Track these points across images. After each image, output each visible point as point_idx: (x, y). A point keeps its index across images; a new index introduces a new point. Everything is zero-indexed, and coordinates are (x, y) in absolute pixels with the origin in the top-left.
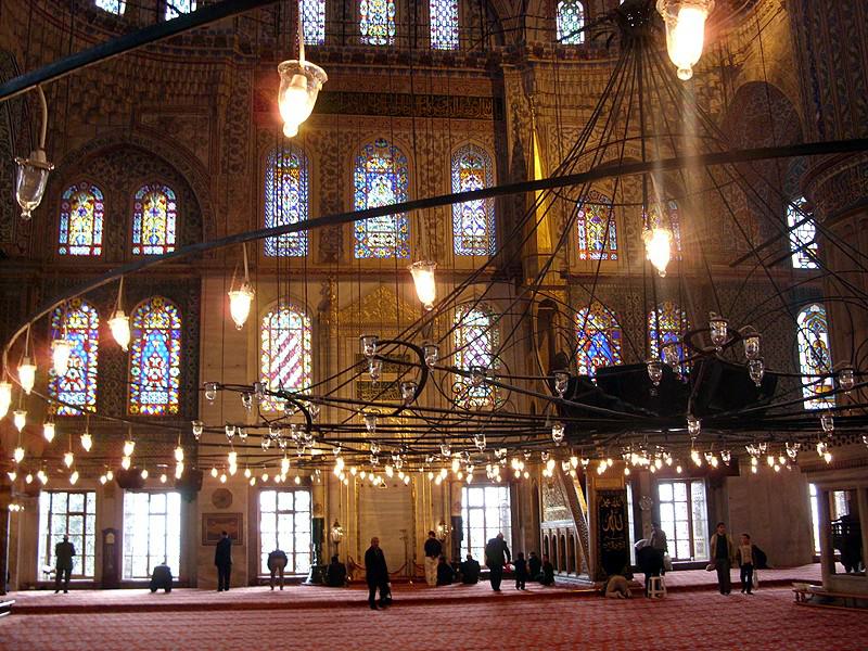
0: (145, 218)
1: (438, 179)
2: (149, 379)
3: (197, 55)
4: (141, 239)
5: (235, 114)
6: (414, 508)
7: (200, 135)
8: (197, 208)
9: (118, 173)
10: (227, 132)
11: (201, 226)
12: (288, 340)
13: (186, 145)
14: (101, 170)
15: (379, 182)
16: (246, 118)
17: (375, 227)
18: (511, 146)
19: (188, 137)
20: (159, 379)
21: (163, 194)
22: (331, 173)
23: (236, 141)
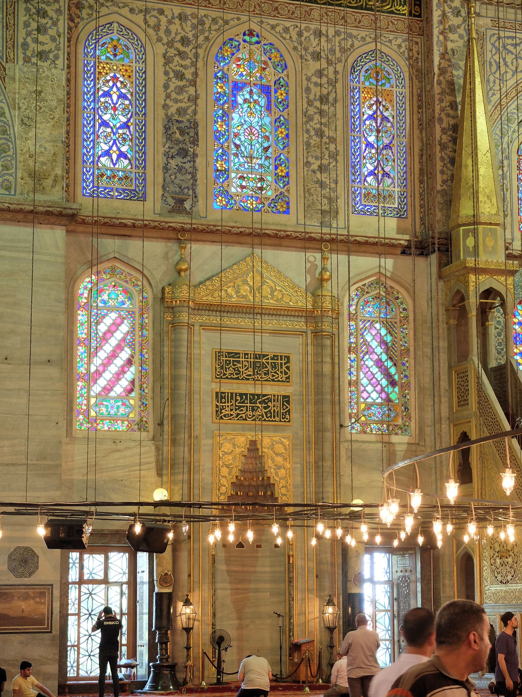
1: (331, 99)
12: (116, 325)
15: (247, 96)
22: (180, 76)
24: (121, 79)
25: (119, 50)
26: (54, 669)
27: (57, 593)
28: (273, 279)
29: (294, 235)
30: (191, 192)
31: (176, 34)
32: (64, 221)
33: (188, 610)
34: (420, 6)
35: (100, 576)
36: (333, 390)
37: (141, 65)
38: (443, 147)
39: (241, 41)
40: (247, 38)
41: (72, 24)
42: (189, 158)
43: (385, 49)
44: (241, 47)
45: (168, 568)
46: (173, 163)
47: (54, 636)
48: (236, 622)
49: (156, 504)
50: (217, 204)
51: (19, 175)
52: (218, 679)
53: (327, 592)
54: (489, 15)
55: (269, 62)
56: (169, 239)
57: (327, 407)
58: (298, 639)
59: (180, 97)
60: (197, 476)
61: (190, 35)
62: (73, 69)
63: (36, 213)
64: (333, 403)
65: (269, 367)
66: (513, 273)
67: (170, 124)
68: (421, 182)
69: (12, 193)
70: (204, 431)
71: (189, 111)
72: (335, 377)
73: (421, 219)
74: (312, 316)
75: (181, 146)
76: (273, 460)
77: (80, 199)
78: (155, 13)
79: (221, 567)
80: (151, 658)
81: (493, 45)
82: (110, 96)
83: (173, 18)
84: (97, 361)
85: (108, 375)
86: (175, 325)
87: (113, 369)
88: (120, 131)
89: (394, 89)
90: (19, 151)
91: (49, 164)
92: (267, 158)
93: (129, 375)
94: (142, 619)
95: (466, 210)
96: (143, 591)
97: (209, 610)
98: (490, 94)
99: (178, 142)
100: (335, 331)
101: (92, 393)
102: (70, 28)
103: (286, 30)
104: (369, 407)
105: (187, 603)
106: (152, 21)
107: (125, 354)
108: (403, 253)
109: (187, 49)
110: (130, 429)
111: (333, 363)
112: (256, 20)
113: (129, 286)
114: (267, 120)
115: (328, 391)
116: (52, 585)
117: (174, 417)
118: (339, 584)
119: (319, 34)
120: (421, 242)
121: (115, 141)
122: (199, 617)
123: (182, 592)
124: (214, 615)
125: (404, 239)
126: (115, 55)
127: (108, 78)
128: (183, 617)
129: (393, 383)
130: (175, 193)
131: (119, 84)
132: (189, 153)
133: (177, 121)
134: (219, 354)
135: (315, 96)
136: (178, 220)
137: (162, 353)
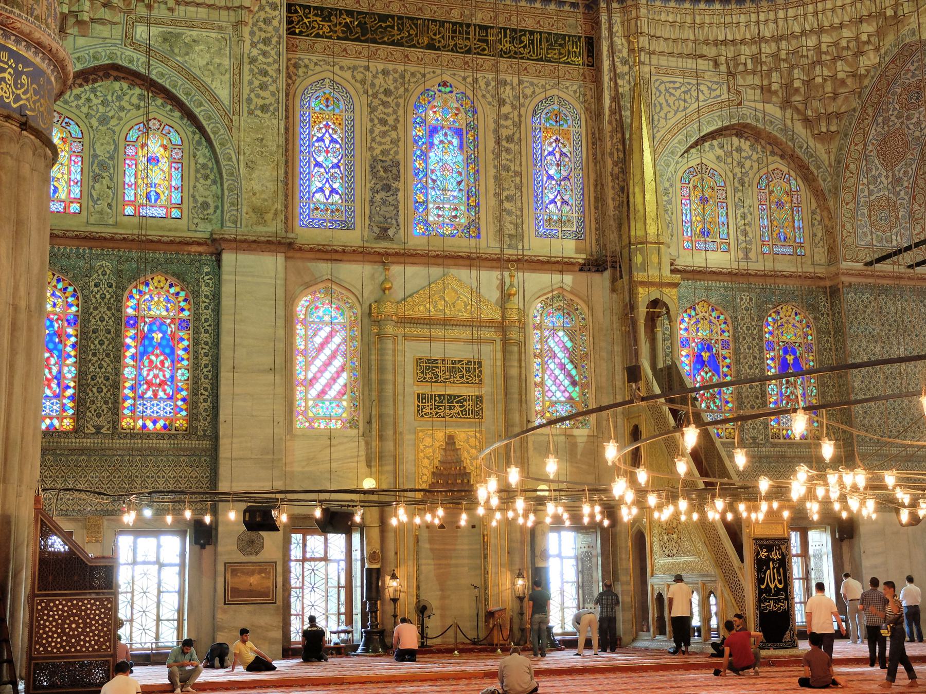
2: (149, 384)
5: (263, 35)
6: (485, 557)
7: (217, 60)
9: (103, 103)
10: (253, 61)
12: (330, 336)
13: (198, 73)
14: (78, 97)
15: (442, 138)
16: (279, 43)
18: (607, 102)
19: (202, 62)
20: (162, 384)
22: (383, 122)
23: (265, 73)
25: (331, 102)
26: (278, 634)
27: (280, 569)
28: (466, 294)
29: (484, 256)
30: (394, 222)
31: (380, 87)
32: (283, 249)
33: (394, 583)
34: (592, 57)
35: (321, 555)
36: (520, 392)
37: (350, 114)
38: (615, 177)
40: (443, 89)
41: (290, 81)
42: (391, 192)
43: (562, 95)
45: (377, 547)
46: (378, 197)
47: (278, 606)
48: (439, 593)
49: (365, 492)
50: (419, 230)
51: (244, 210)
52: (423, 643)
53: (517, 567)
55: (461, 108)
56: (376, 262)
57: (515, 405)
58: (492, 607)
59: (384, 140)
60: (401, 467)
61: (392, 88)
62: (291, 119)
64: (521, 401)
65: (464, 372)
66: (676, 285)
68: (596, 208)
70: (406, 428)
71: (392, 152)
72: (523, 379)
73: (597, 240)
74: (502, 327)
75: (385, 182)
76: (468, 452)
77: (297, 229)
78: (362, 69)
79: (425, 546)
80: (364, 625)
81: (657, 89)
82: (323, 141)
83: (377, 73)
84: (314, 369)
85: (323, 381)
86: (381, 337)
87: (327, 375)
88: (332, 171)
89: (571, 129)
90: (244, 190)
91: (270, 201)
92: (460, 190)
93: (342, 381)
94: (356, 591)
95: (636, 231)
96: (357, 567)
97: (414, 583)
98: (655, 131)
99: (382, 179)
100: (522, 339)
101: (309, 396)
102: (288, 85)
104: (553, 404)
105: (394, 577)
106: (359, 77)
107: (338, 363)
108: (581, 270)
109: (390, 100)
110: (344, 427)
111: (520, 367)
112: (449, 73)
113: (341, 304)
114: (460, 158)
115: (515, 389)
116: (276, 563)
117: (381, 416)
118: (528, 559)
120: (596, 260)
122: (405, 589)
123: (389, 568)
124: (418, 587)
125: (581, 258)
126: (327, 106)
127: (321, 126)
128: (391, 590)
129: (574, 383)
130: (380, 222)
131: (331, 131)
134: (419, 361)
136: (382, 246)
137: (370, 360)
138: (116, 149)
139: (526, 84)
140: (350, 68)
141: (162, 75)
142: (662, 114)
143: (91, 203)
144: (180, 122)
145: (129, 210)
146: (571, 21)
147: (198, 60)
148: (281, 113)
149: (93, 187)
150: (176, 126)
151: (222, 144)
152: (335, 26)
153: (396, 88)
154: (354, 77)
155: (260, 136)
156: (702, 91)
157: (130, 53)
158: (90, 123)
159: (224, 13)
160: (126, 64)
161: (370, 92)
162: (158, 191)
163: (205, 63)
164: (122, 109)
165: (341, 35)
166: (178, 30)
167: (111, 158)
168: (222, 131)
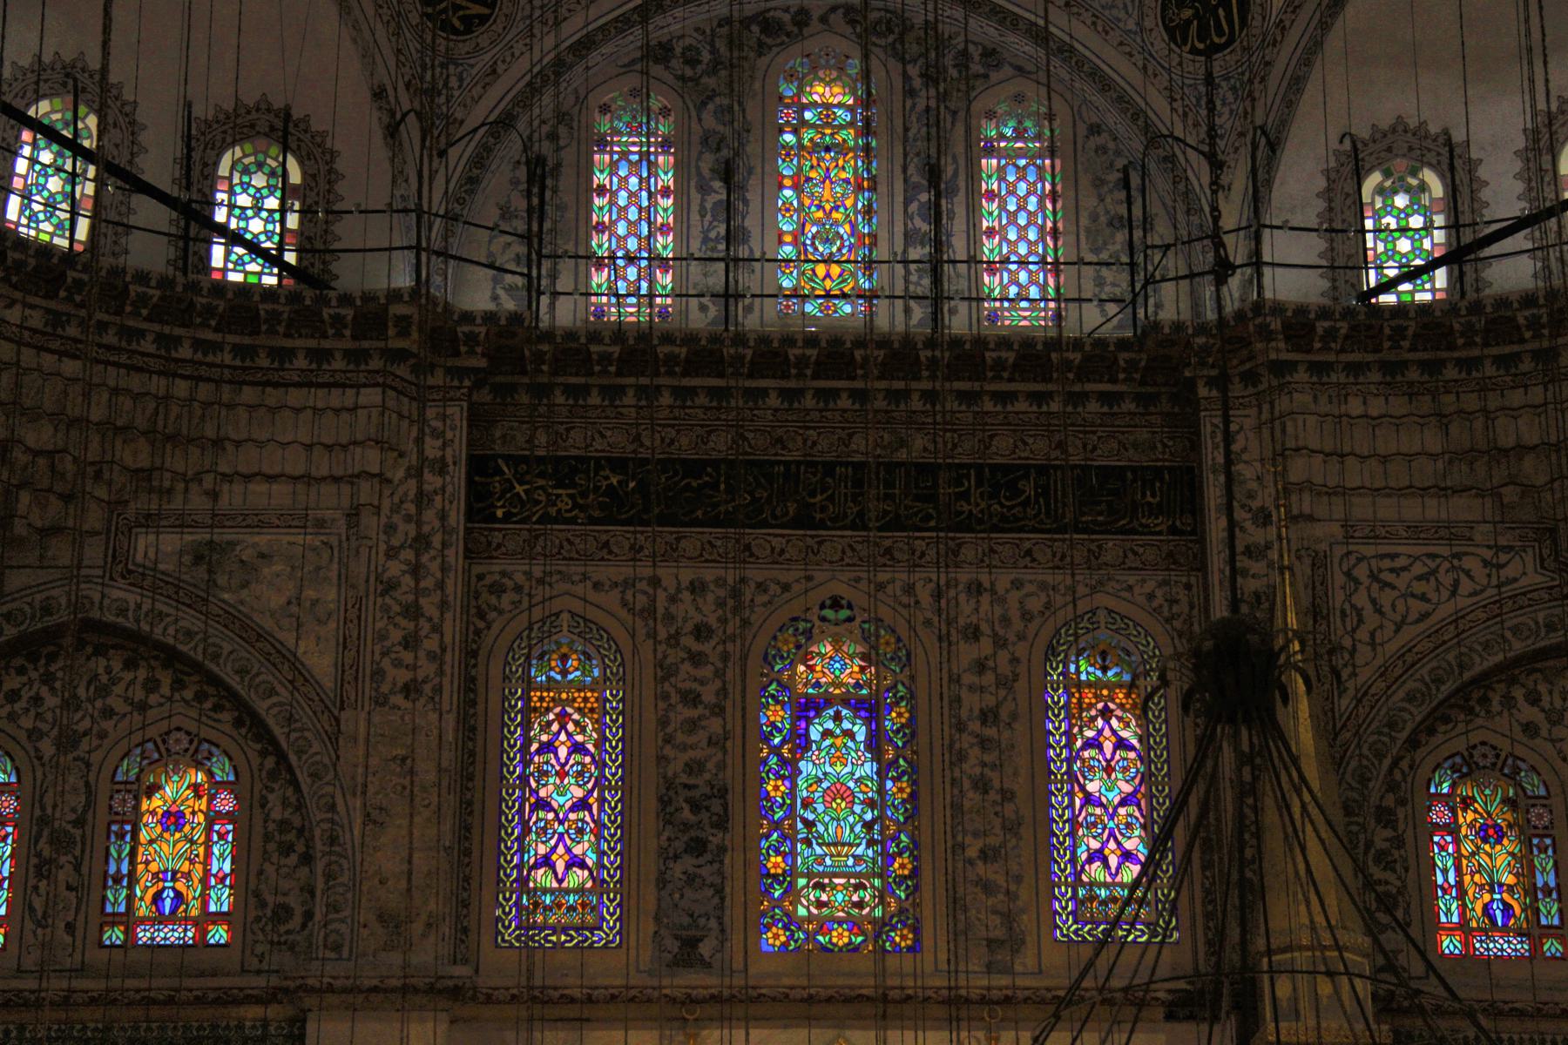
0: (144, 835)
1: (1004, 714)
3: (301, 362)
4: (130, 898)
7: (310, 593)
8: (300, 807)
10: (390, 587)
11: (307, 859)
13: (268, 624)
15: (830, 725)
17: (820, 860)
19: (277, 601)
21: (198, 765)
22: (691, 698)
24: (576, 716)
30: (713, 923)
31: (685, 620)
39: (815, 619)
40: (829, 613)
41: (481, 625)
42: (708, 856)
44: (816, 631)
46: (678, 869)
54: (1335, 516)
61: (712, 621)
63: (385, 991)
67: (671, 793)
69: (345, 954)
71: (710, 765)
75: (693, 833)
78: (643, 585)
81: (1348, 574)
83: (679, 590)
92: (870, 843)
99: (686, 826)
103: (909, 589)
108: (1170, 1017)
119: (976, 589)
121: (561, 835)
131: (571, 727)
132: (710, 847)
133: (686, 786)
135: (971, 710)
138: (90, 803)
139: (1029, 588)
140: (616, 585)
141: (189, 634)
142: (1362, 634)
143: (29, 925)
144: (235, 733)
145: (116, 935)
146: (1143, 435)
147: (267, 598)
148: (450, 696)
149: (36, 888)
150: (225, 742)
151: (315, 776)
152: (584, 495)
153: (723, 621)
154: (624, 604)
155: (401, 752)
156: (1468, 573)
157: (121, 594)
158: (37, 750)
159: (328, 489)
160: (110, 618)
161: (662, 634)
162: (180, 886)
163: (283, 600)
164: (108, 713)
165: (596, 514)
166: (229, 535)
167: (80, 822)
168: (316, 747)
